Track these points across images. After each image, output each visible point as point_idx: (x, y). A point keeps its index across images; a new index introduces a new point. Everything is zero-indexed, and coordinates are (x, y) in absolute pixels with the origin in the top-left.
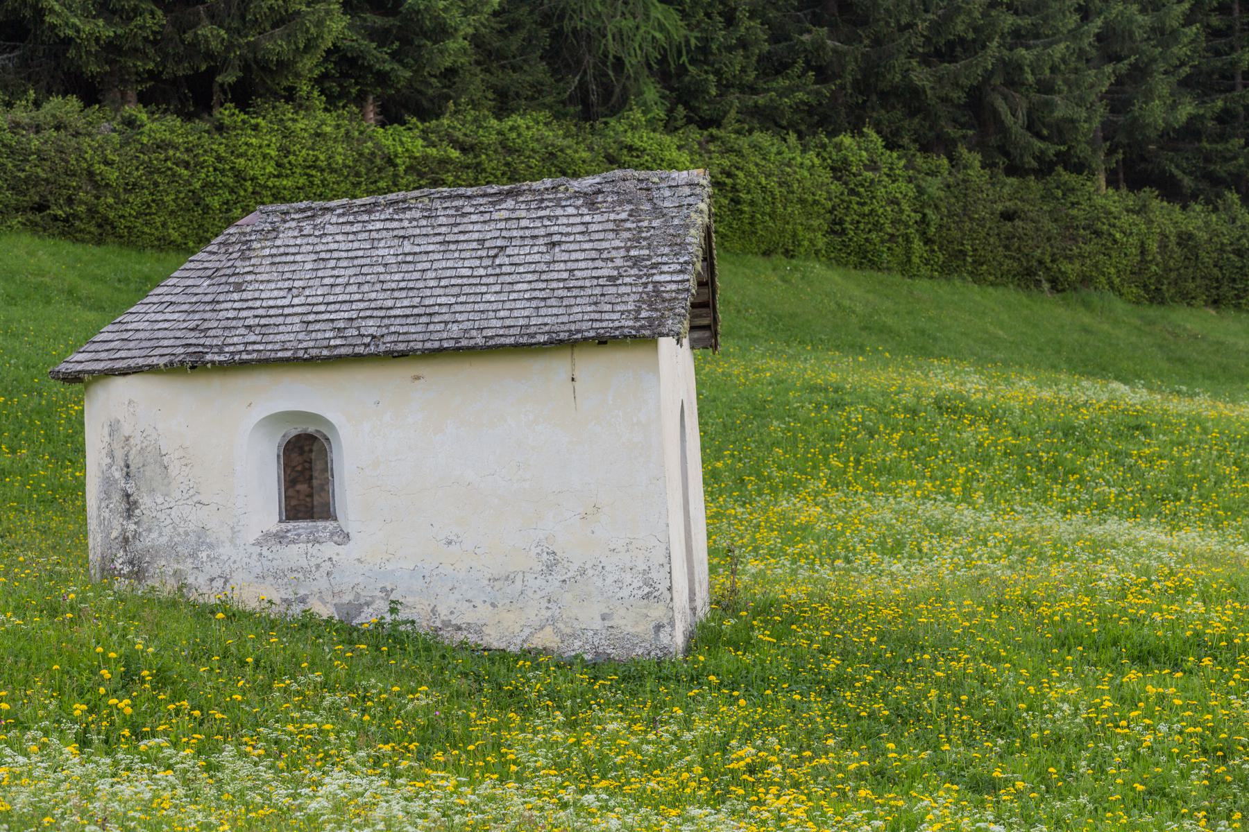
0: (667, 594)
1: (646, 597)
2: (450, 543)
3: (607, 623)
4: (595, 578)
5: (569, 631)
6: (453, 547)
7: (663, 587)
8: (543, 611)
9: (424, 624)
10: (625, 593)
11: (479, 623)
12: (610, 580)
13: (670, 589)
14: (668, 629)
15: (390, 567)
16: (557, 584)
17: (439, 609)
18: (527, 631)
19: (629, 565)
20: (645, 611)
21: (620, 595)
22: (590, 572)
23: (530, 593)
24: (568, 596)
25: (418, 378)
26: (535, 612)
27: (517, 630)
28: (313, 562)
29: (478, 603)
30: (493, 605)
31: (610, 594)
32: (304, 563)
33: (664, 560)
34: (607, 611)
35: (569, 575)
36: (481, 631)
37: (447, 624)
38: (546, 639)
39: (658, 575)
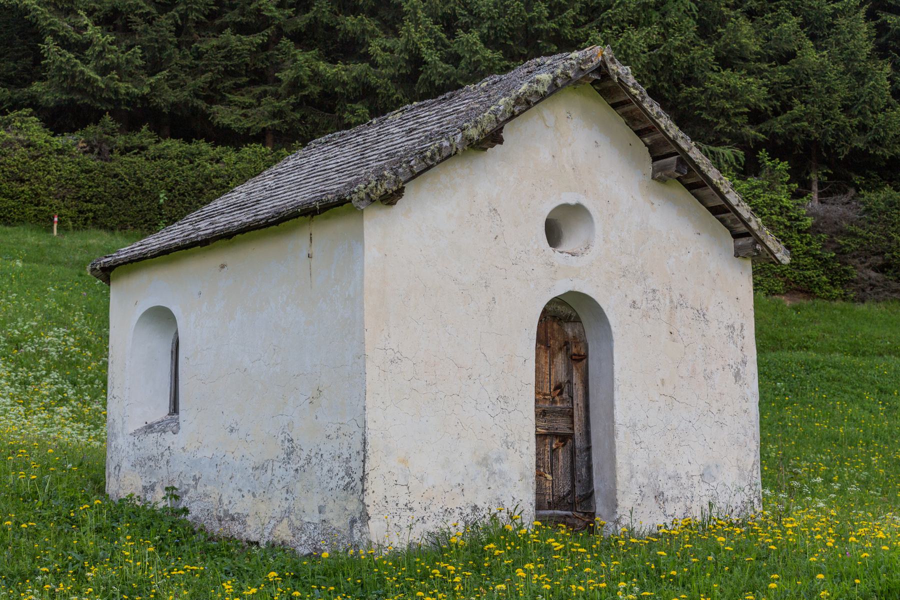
0: (359, 483)
1: (345, 488)
2: (232, 431)
3: (323, 517)
4: (316, 467)
5: (297, 524)
6: (234, 435)
7: (357, 476)
8: (284, 502)
9: (214, 513)
10: (333, 484)
11: (245, 513)
12: (326, 469)
13: (363, 479)
14: (359, 524)
15: (199, 456)
16: (293, 472)
17: (223, 498)
18: (273, 522)
19: (338, 453)
20: (344, 503)
21: (331, 486)
22: (314, 460)
23: (275, 482)
24: (299, 485)
25: (223, 266)
26: (278, 505)
27: (267, 522)
28: (161, 449)
29: (245, 492)
30: (254, 496)
31: (325, 485)
32: (155, 452)
33: (359, 447)
34: (322, 503)
35: (302, 462)
36: (244, 523)
37: (226, 513)
38: (283, 533)
39: (355, 464)
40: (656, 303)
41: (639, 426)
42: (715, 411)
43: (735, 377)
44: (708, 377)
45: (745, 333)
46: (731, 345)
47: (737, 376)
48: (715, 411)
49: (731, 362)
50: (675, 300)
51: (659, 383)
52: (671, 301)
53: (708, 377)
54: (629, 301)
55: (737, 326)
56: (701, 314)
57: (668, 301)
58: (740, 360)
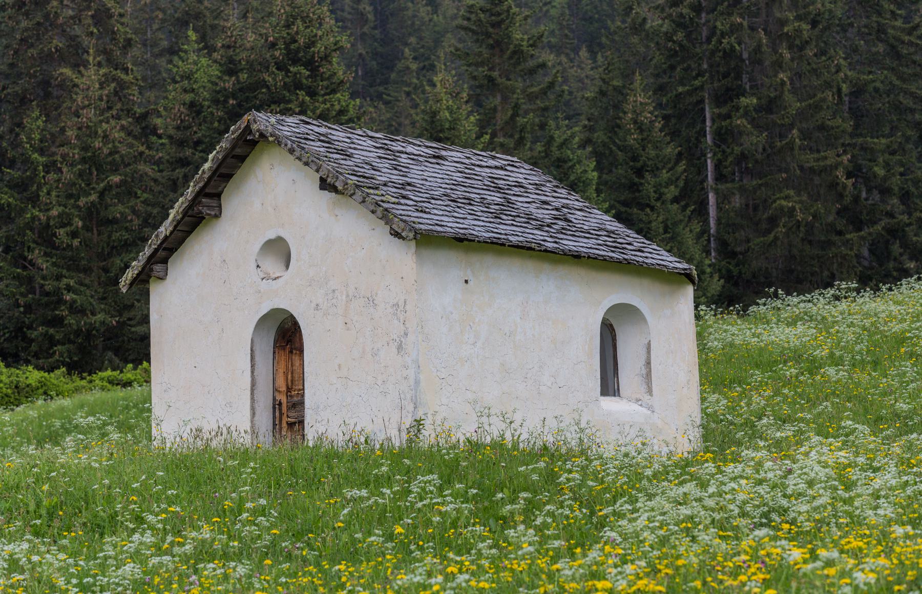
40: (334, 301)
41: (321, 407)
42: (379, 383)
43: (398, 349)
44: (375, 355)
45: (407, 307)
46: (396, 321)
47: (400, 348)
48: (379, 383)
49: (395, 337)
50: (351, 294)
51: (337, 368)
52: (348, 296)
53: (375, 355)
54: (313, 305)
55: (401, 303)
56: (371, 301)
57: (344, 297)
58: (402, 333)
